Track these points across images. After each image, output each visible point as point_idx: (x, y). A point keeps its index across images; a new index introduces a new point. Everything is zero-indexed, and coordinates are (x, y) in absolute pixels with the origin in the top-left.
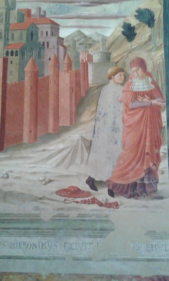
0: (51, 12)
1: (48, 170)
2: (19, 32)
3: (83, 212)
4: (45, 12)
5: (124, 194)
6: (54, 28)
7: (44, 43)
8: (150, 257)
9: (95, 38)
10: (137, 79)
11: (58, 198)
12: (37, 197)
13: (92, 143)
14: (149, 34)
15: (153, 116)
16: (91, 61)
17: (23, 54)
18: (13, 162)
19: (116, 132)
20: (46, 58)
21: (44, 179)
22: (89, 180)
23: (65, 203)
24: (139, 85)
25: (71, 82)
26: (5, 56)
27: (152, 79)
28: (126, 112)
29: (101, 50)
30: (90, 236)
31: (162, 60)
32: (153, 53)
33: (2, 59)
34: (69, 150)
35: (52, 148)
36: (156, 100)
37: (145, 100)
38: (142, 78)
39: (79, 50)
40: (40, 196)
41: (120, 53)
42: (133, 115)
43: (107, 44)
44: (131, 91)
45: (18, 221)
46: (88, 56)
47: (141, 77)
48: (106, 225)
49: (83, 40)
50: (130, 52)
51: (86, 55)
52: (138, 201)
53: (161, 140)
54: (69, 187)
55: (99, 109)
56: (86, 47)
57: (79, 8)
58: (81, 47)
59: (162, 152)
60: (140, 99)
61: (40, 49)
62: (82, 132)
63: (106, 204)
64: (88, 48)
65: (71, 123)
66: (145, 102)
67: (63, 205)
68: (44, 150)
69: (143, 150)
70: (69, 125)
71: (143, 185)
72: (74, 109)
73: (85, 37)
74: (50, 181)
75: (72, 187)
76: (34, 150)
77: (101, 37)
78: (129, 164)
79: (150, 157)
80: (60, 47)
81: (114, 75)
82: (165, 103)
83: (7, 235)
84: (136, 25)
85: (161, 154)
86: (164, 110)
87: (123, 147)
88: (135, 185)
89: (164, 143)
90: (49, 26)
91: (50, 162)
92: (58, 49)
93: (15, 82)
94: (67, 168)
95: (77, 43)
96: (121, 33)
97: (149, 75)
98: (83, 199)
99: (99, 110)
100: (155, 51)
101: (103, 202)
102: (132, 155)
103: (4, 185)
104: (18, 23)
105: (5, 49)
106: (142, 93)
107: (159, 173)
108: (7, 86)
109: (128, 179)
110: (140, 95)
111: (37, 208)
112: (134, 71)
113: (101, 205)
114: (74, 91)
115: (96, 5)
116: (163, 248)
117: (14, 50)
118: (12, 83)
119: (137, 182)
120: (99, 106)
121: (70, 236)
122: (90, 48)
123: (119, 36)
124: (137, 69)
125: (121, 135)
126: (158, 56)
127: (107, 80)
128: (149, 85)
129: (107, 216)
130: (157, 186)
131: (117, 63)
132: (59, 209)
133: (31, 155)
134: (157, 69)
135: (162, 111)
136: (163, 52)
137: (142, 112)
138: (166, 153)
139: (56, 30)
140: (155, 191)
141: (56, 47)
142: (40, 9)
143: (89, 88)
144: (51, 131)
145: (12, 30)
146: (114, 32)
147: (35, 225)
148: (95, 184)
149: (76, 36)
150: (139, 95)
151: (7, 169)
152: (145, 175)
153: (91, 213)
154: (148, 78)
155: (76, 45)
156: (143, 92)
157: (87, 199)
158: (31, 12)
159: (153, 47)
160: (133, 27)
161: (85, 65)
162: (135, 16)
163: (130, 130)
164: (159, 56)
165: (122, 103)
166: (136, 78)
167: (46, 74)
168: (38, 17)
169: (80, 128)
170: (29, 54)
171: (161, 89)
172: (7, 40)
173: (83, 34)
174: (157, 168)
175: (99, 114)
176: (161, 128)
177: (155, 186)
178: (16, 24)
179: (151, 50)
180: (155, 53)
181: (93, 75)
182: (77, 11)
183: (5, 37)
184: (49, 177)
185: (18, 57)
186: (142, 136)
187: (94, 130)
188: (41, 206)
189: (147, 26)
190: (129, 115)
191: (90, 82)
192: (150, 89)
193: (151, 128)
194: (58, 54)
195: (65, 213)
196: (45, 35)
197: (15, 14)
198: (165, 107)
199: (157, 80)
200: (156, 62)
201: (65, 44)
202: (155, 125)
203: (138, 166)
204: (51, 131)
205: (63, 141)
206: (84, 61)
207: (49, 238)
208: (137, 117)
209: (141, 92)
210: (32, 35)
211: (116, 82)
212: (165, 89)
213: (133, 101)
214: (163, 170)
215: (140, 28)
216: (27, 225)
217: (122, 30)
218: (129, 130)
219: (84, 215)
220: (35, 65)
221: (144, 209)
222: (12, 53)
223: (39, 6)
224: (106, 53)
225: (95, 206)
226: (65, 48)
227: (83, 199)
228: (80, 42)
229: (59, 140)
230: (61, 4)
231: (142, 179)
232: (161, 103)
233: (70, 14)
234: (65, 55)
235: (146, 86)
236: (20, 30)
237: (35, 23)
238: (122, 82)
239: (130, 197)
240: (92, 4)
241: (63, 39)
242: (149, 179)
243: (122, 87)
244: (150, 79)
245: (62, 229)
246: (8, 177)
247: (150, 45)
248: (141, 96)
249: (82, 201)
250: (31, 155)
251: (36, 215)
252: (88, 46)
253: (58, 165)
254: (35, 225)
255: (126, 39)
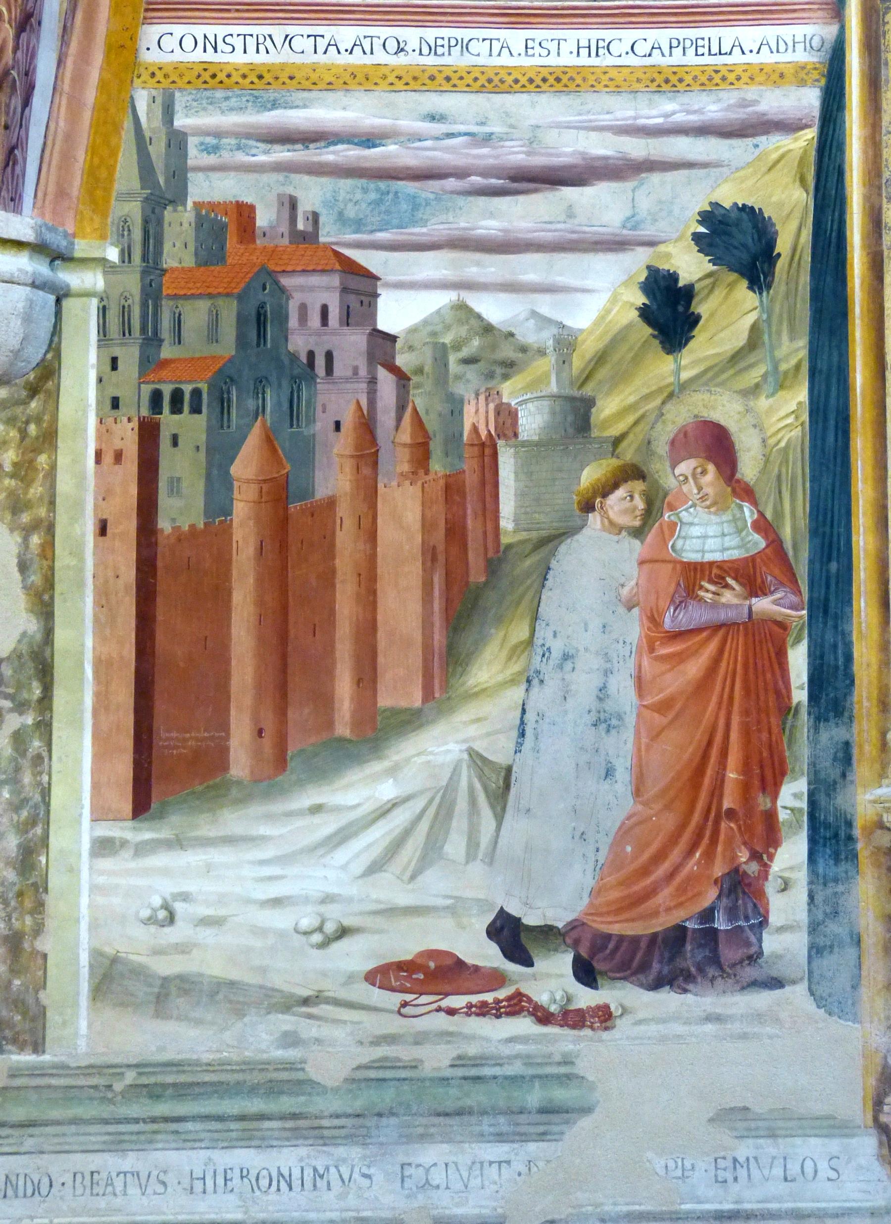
0: (341, 218)
1: (334, 890)
2: (203, 305)
3: (472, 1050)
4: (315, 217)
5: (634, 974)
6: (357, 292)
7: (311, 355)
8: (727, 1206)
9: (529, 335)
10: (698, 508)
11: (377, 996)
12: (292, 995)
13: (513, 778)
14: (752, 318)
15: (756, 664)
16: (510, 433)
17: (223, 403)
18: (193, 858)
19: (608, 731)
20: (321, 425)
21: (316, 923)
22: (498, 924)
23: (405, 1016)
24: (705, 537)
25: (427, 526)
26: (145, 412)
27: (759, 511)
28: (652, 649)
29: (553, 388)
30: (500, 1137)
31: (800, 428)
32: (763, 403)
33: (135, 424)
34: (418, 805)
35: (348, 798)
36: (771, 598)
37: (727, 597)
38: (718, 505)
39: (459, 389)
40: (306, 993)
41: (632, 399)
42: (679, 658)
43: (577, 363)
44: (675, 562)
45: (220, 1089)
46: (498, 413)
47: (714, 503)
48: (560, 1095)
49: (476, 342)
50: (671, 396)
51: (492, 406)
52: (689, 998)
53: (782, 762)
54: (421, 954)
55: (543, 634)
56: (490, 376)
57: (461, 201)
58: (471, 373)
59: (785, 808)
60: (708, 591)
61: (296, 380)
62: (472, 731)
63: (566, 1013)
64: (499, 378)
65: (428, 694)
66: (725, 606)
67: (395, 1025)
68: (317, 809)
69: (715, 801)
70: (418, 704)
71: (710, 936)
72: (439, 638)
73: (488, 329)
74: (343, 932)
75: (432, 954)
76: (278, 807)
77: (554, 330)
78: (659, 857)
79: (739, 828)
80: (382, 373)
81: (605, 495)
82: (803, 609)
83: (174, 1145)
84: (700, 280)
85: (783, 815)
86: (798, 640)
87: (637, 792)
88: (679, 934)
89: (793, 770)
90: (335, 280)
91: (342, 855)
92: (373, 381)
93: (192, 526)
94: (413, 878)
95: (453, 358)
96: (634, 314)
97: (746, 493)
98: (475, 999)
99: (540, 642)
100: (773, 394)
101: (553, 1008)
102: (669, 821)
103: (158, 952)
104: (199, 265)
105: (144, 382)
106: (715, 571)
107: (771, 888)
108: (156, 544)
109: (655, 914)
110: (707, 578)
111: (290, 1039)
112: (686, 478)
113: (544, 1017)
114: (441, 558)
115: (536, 191)
116: (778, 1171)
117: (183, 387)
118: (176, 529)
119: (687, 924)
120: (544, 625)
121: (424, 1138)
122: (506, 377)
123: (629, 327)
124: (699, 470)
125: (630, 745)
126: (782, 413)
127: (578, 512)
128: (744, 533)
129: (567, 1061)
130: (760, 940)
131: (617, 441)
132: (378, 1041)
133: (264, 830)
134: (776, 470)
135: (790, 640)
136: (802, 394)
137: (712, 647)
138: (800, 810)
139: (363, 298)
140: (754, 958)
141: (363, 372)
142: (293, 204)
143: (502, 548)
144: (343, 729)
145: (175, 297)
146: (601, 318)
147: (287, 1104)
148: (524, 939)
149: (448, 328)
150: (702, 578)
151: (167, 887)
152: (719, 897)
153: (507, 1050)
154: (741, 508)
155: (446, 365)
156: (720, 565)
157: (489, 997)
158: (254, 218)
159: (765, 376)
160: (685, 286)
161: (487, 451)
162: (697, 238)
163: (665, 721)
164: (787, 416)
165: (636, 611)
166: (694, 505)
167: (321, 492)
168: (286, 241)
169: (464, 714)
170: (251, 404)
171: (790, 553)
172: (151, 341)
173: (479, 317)
174: (765, 868)
175: (543, 655)
176: (785, 708)
177: (753, 939)
178: (190, 270)
179: (754, 390)
180: (771, 400)
181: (521, 495)
182: (450, 215)
183: (144, 329)
184: (335, 915)
185: (201, 420)
186: (710, 743)
187: (522, 722)
188: (310, 1030)
189: (744, 283)
190: (663, 659)
191: (506, 523)
192: (747, 551)
193: (746, 713)
194: (372, 402)
195: (404, 1053)
196: (315, 320)
197: (186, 225)
198: (801, 629)
199: (779, 514)
200: (772, 441)
201: (401, 361)
202: (762, 698)
203: (692, 866)
204: (343, 729)
205: (393, 771)
206: (483, 434)
207: (341, 1151)
208: (694, 668)
209: (711, 564)
210: (261, 320)
211: (611, 523)
212: (805, 555)
213: (681, 602)
214: (786, 875)
215: (717, 292)
216: (255, 1105)
217: (641, 299)
218: (659, 720)
219: (479, 1061)
220: (274, 450)
221: (709, 1028)
222: (177, 399)
223: (290, 190)
224: (571, 399)
225: (524, 1025)
226: (401, 377)
227: (475, 999)
228: (465, 352)
229: (376, 767)
230: (382, 185)
231: (708, 915)
232: (789, 611)
233: (424, 230)
234: (401, 408)
235: (731, 541)
236: (210, 296)
237: (272, 267)
238: (637, 523)
239: (656, 986)
240: (516, 185)
241: (392, 339)
242: (732, 913)
243: (637, 543)
244: (749, 513)
245: (392, 1114)
246: (171, 919)
247: (751, 366)
248: (711, 581)
249: (470, 1006)
250: (264, 830)
251: (290, 1066)
252: (499, 371)
253: (374, 868)
254: (287, 1104)
255: (656, 342)
